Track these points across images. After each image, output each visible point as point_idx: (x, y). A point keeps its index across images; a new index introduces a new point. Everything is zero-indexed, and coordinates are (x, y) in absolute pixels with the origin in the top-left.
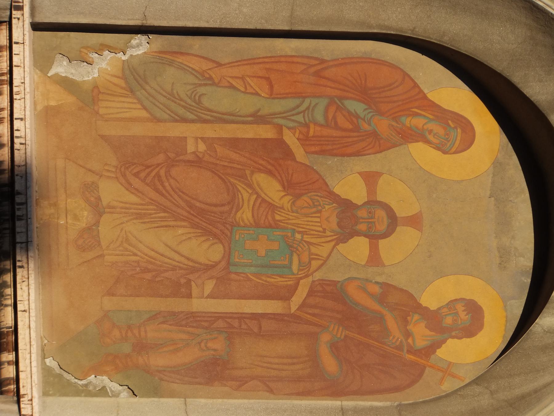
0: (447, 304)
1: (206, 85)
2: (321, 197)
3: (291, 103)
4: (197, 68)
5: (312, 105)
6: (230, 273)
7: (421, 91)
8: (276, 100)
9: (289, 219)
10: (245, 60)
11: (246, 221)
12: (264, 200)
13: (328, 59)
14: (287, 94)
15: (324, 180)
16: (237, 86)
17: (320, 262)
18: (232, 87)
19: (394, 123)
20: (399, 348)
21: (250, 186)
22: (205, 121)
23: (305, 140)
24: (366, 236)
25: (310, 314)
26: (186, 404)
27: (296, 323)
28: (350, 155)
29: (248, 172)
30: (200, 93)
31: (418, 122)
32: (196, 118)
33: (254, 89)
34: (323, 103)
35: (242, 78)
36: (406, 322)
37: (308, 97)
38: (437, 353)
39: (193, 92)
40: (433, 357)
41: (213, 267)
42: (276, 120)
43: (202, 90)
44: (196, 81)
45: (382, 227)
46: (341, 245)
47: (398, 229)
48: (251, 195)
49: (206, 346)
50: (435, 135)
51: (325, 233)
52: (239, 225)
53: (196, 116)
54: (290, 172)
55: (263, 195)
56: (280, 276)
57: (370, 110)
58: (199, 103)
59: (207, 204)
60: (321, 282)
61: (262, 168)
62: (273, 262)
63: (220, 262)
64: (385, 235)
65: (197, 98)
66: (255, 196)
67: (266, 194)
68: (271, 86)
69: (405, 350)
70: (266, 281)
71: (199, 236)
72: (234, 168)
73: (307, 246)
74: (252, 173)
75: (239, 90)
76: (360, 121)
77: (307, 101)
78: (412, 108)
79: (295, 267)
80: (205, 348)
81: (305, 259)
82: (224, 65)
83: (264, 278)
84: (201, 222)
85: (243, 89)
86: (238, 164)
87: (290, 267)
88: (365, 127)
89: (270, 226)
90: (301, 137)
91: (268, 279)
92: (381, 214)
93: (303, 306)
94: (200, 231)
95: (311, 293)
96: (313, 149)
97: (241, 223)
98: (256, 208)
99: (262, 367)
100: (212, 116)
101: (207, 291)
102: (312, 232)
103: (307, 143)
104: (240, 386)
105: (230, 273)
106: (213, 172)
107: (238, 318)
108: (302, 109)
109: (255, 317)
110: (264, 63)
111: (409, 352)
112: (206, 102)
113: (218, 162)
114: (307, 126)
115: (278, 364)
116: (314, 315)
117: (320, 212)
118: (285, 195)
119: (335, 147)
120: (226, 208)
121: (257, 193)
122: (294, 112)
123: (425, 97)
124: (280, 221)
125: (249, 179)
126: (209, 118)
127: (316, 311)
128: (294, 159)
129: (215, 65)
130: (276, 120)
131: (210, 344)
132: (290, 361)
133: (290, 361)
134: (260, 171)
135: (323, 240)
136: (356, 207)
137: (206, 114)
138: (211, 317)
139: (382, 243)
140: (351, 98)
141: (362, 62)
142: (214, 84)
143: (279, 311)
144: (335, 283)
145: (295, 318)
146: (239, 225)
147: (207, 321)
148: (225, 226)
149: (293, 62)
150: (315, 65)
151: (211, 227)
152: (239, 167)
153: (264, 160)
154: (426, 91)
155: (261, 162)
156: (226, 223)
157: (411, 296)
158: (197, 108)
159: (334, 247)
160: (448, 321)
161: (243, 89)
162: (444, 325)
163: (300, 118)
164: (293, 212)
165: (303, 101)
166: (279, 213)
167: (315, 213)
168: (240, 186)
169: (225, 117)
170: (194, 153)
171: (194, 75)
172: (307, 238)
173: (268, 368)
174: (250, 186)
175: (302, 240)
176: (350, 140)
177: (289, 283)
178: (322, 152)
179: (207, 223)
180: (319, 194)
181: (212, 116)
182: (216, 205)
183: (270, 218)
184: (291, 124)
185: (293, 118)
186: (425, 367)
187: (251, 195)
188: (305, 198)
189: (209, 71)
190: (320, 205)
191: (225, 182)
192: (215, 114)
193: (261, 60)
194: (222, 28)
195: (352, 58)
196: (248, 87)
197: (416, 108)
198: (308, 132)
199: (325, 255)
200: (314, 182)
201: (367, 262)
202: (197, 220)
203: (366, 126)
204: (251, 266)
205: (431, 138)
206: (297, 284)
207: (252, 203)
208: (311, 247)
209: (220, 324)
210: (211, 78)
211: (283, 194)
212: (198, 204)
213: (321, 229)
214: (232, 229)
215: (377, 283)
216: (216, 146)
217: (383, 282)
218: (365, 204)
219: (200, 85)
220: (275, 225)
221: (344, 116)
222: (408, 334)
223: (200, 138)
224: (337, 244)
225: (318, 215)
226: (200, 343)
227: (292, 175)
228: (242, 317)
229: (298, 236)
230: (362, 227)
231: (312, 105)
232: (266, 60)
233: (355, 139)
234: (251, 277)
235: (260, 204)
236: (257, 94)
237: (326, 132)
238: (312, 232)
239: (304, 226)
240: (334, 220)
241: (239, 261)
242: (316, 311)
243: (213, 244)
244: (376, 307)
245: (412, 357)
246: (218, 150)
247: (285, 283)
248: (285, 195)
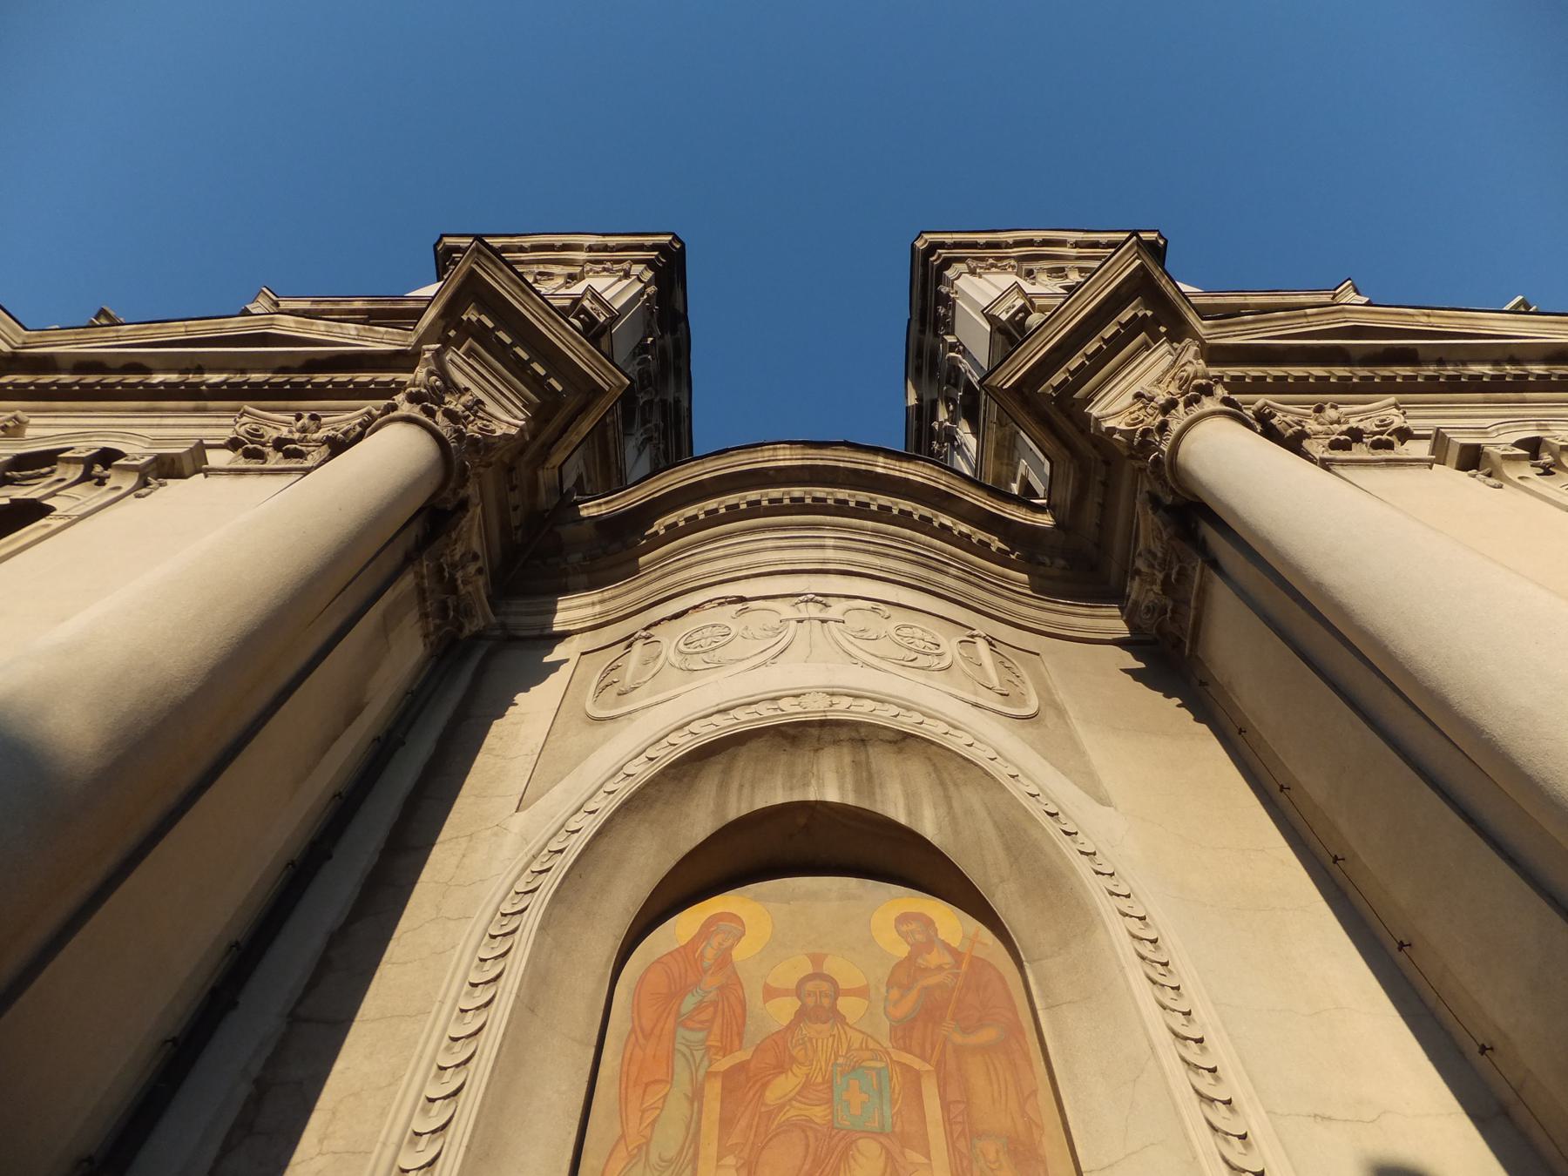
0: (903, 937)
1: (647, 1153)
2: (793, 1038)
3: (680, 1064)
4: (624, 1163)
5: (684, 1041)
6: (893, 1132)
7: (677, 950)
8: (675, 1077)
9: (821, 1069)
10: (621, 1109)
11: (826, 1113)
12: (799, 1093)
13: (631, 1025)
14: (668, 1065)
15: (773, 1034)
16: (652, 1118)
17: (869, 1038)
18: (654, 1121)
19: (711, 972)
20: (956, 976)
21: (781, 1107)
22: (696, 1156)
23: (726, 1051)
24: (836, 999)
25: (932, 1052)
26: (1090, 1172)
27: (945, 1065)
28: (744, 1010)
29: (763, 1110)
30: (658, 1160)
31: (710, 954)
32: (690, 1167)
33: (659, 1099)
34: (681, 1032)
35: (643, 1112)
36: (926, 969)
37: (674, 1045)
38: (955, 946)
39: (656, 1169)
40: (960, 950)
41: (888, 1152)
42: (700, 1078)
43: (654, 1158)
44: (641, 1165)
45: (825, 986)
46: (847, 1021)
47: (825, 972)
48: (792, 1106)
49: (994, 1163)
50: (724, 941)
51: (834, 1035)
52: (832, 1121)
53: (687, 1166)
54: (763, 1065)
55: (793, 1094)
56: (891, 1080)
57: (694, 991)
58: (670, 1161)
59: (805, 1157)
60: (893, 1040)
61: (758, 1094)
62: (875, 1087)
63: (881, 1143)
64: (833, 982)
65: (663, 1164)
66: (794, 1102)
67: (791, 1091)
68: (656, 1082)
69: (958, 971)
70: (899, 1094)
71: (849, 1167)
72: (758, 1124)
73: (853, 1052)
74: (764, 1104)
75: (659, 1115)
76: (705, 1000)
77: (678, 1046)
78: (694, 956)
79: (879, 1065)
80: (997, 1164)
81: (867, 1054)
82: (623, 1131)
83: (896, 1096)
84: (830, 1165)
85: (658, 1112)
86: (753, 1119)
87: (879, 1071)
88: (712, 996)
89: (831, 1088)
90: (721, 1053)
91: (897, 1091)
92: (809, 986)
93: (923, 1058)
94: (842, 1165)
95: (908, 1050)
96: (736, 1043)
97: (827, 1118)
98: (807, 1101)
99: (1007, 1101)
100: (690, 1147)
101: (923, 1160)
102: (835, 1045)
103: (728, 1048)
104: (1037, 1126)
105: (893, 1132)
106: (763, 1148)
107: (950, 1124)
108: (687, 1051)
109: (945, 1106)
110: (627, 1088)
111: (959, 967)
112: (671, 1153)
113: (750, 1142)
114: (708, 1048)
115: (999, 1085)
116: (933, 1049)
117: (810, 1039)
118: (792, 1071)
119: (734, 1023)
120: (810, 1134)
121: (790, 1100)
122: (691, 1059)
123: (684, 947)
124: (823, 1078)
125: (772, 1108)
126: (691, 1150)
127: (928, 1046)
128: (748, 1062)
129: (623, 1142)
130: (700, 1078)
131: (992, 1156)
132: (992, 1073)
133: (992, 1073)
134: (762, 1096)
135: (843, 1036)
136: (803, 1005)
137: (687, 1153)
138: (954, 1155)
139: (843, 985)
140: (680, 1004)
141: (639, 995)
142: (648, 1143)
143: (934, 1081)
144: (893, 1029)
145: (940, 1067)
146: (832, 1121)
147: (961, 1160)
148: (834, 1136)
149: (630, 1059)
150: (637, 1038)
151: (836, 1153)
152: (756, 1119)
153: (749, 1091)
154: (677, 946)
155: (751, 1093)
156: (830, 1134)
157: (899, 964)
158: (677, 1164)
159: (850, 1027)
160: (919, 937)
161: (658, 1112)
162: (925, 940)
163: (698, 1055)
164: (812, 1065)
165: (679, 1050)
166: (814, 1078)
167: (812, 1043)
168: (781, 1118)
169: (691, 1131)
170: (737, 1170)
171: (632, 1167)
172: (843, 1052)
173: (1007, 1095)
174: (781, 1107)
175: (844, 1056)
176: (726, 1009)
177: (898, 1070)
178: (740, 1035)
179: (831, 1157)
180: (790, 1039)
181: (690, 1147)
182: (807, 1146)
183: (821, 1087)
184: (706, 1063)
185: (697, 1061)
186: (973, 956)
187: (792, 1106)
188: (794, 1053)
189: (630, 1149)
190: (803, 1039)
191: (777, 1134)
192: (687, 1145)
193: (623, 1091)
194: (581, 1119)
195: (633, 1005)
196: (656, 1105)
197: (694, 953)
198: (717, 1047)
199: (861, 1036)
200: (776, 1043)
201: (865, 998)
202: (828, 1169)
203: (712, 994)
204: (882, 1109)
205: (727, 944)
206: (898, 1062)
207: (803, 1106)
208: (853, 1048)
209: (962, 1145)
210: (639, 1147)
211: (790, 1073)
212: (806, 1167)
213: (831, 1040)
214: (837, 1128)
215: (887, 992)
216: (728, 1145)
217: (887, 985)
218: (799, 997)
219: (647, 1159)
220: (830, 1084)
221: (698, 1014)
222: (940, 968)
223: (718, 1161)
224: (847, 1024)
225: (814, 1041)
226: (992, 1170)
227: (766, 1063)
228: (948, 1121)
229: (840, 1060)
230: (826, 1002)
231: (684, 1041)
232: (623, 1086)
233: (726, 1004)
234: (896, 1108)
235: (803, 1097)
236: (666, 1095)
237: (716, 1029)
238: (835, 1045)
239: (829, 1054)
240: (820, 1026)
241: (877, 1122)
242: (928, 1046)
243: (858, 1150)
244: (913, 994)
245: (964, 966)
246: (734, 1142)
247: (898, 1074)
248: (792, 1071)
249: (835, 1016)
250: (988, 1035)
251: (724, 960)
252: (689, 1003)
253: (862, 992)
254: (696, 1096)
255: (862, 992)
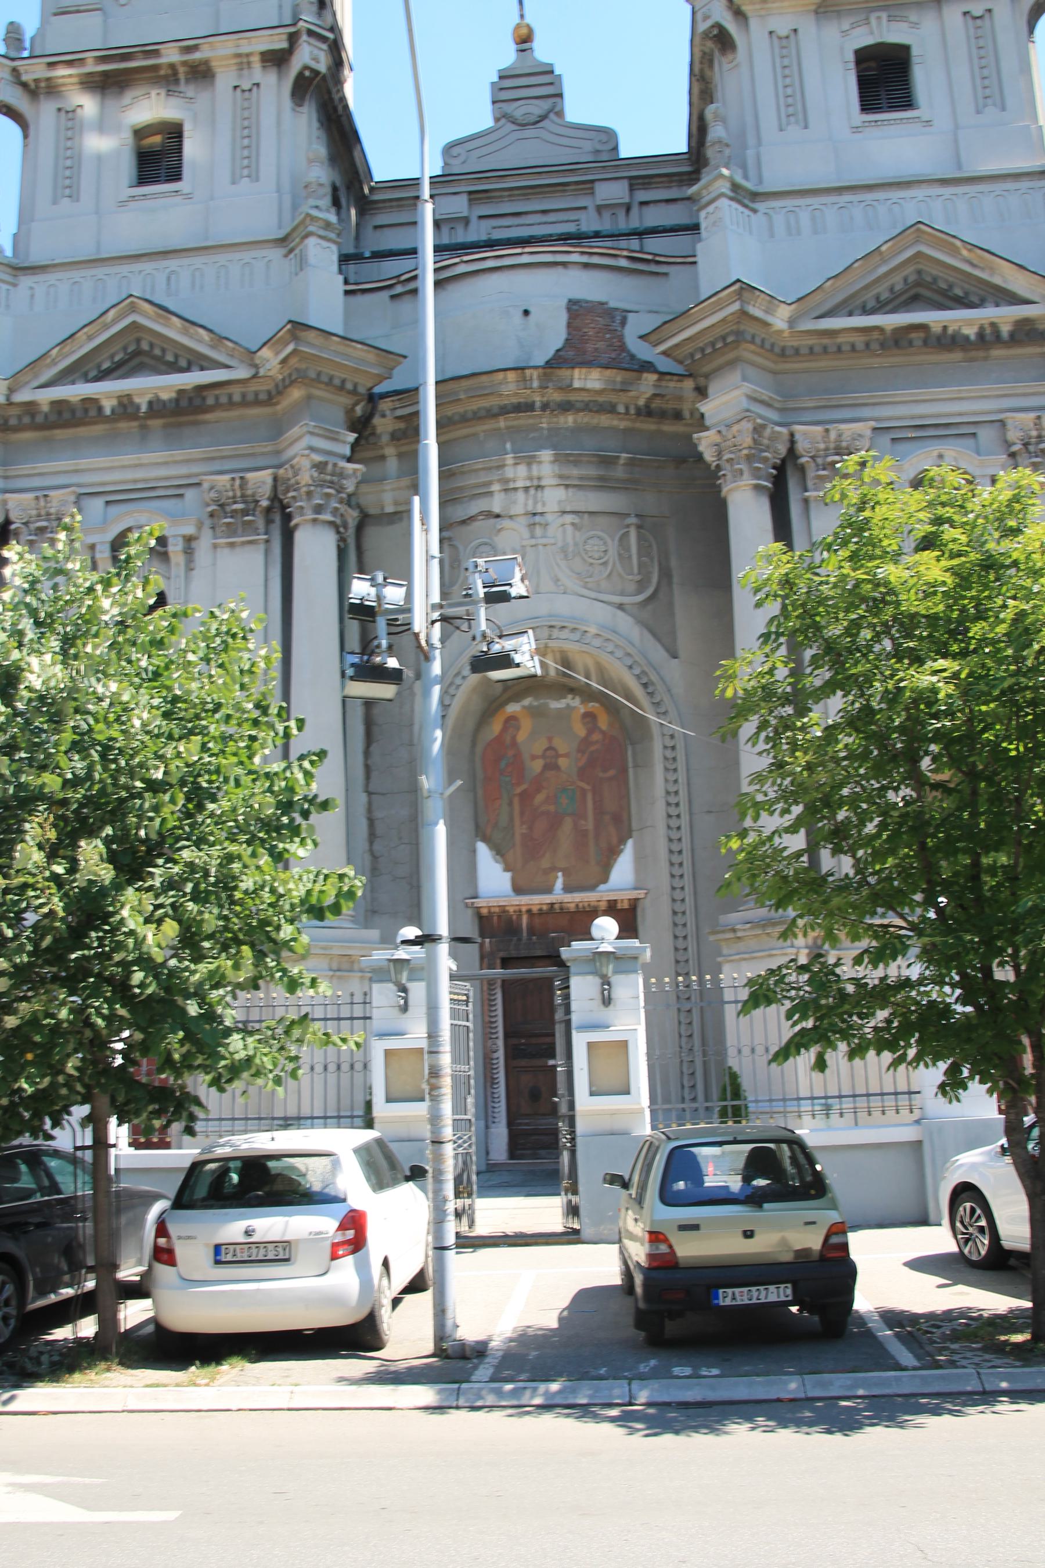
95: (582, 780)
109: (594, 802)
222: (597, 742)
249: (557, 768)
250: (612, 773)
251: (514, 743)
252: (503, 764)
253: (566, 755)
254: (510, 804)
255: (566, 755)
